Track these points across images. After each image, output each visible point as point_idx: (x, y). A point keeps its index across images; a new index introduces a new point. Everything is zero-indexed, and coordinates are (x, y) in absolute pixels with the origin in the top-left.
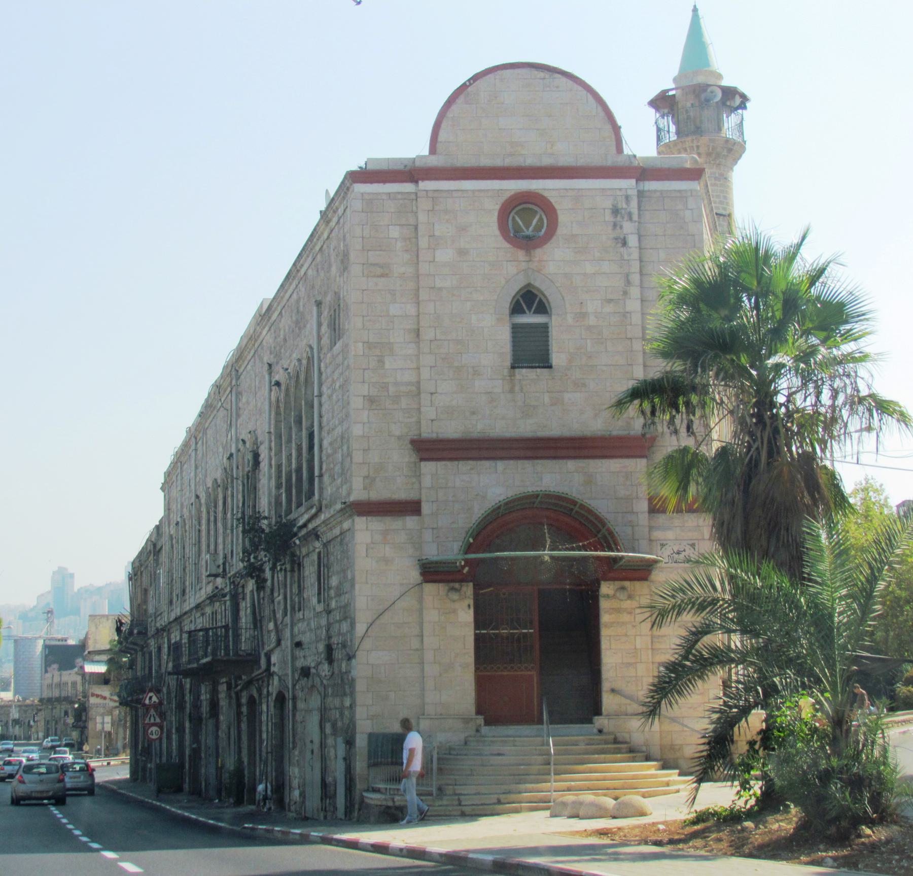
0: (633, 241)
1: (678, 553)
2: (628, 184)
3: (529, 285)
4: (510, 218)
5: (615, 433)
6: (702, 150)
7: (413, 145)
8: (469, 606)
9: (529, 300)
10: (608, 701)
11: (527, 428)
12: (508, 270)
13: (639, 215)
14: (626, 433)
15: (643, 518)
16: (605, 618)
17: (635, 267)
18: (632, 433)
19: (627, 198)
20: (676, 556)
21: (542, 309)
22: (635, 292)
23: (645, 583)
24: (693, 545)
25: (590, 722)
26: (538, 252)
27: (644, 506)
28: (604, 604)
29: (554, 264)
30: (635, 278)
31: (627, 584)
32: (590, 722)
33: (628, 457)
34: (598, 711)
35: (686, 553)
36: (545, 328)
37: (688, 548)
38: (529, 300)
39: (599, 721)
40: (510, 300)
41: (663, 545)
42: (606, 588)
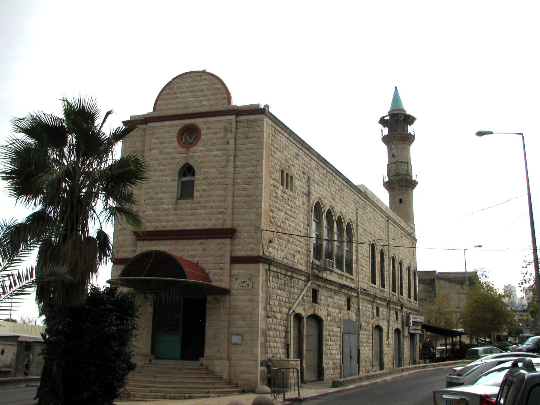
0: (232, 141)
1: (243, 282)
2: (232, 118)
3: (187, 164)
4: (184, 136)
5: (217, 227)
6: (396, 138)
7: (146, 108)
8: (151, 305)
9: (187, 170)
10: (208, 351)
11: (181, 226)
12: (178, 156)
13: (236, 131)
14: (222, 227)
15: (227, 266)
16: (208, 312)
17: (232, 153)
18: (225, 227)
19: (231, 123)
20: (242, 284)
21: (193, 174)
22: (231, 164)
23: (228, 296)
24: (250, 279)
25: (198, 360)
26: (192, 149)
27: (228, 260)
28: (208, 305)
29: (198, 154)
30: (232, 158)
31: (219, 297)
32: (198, 360)
33: (222, 238)
34: (203, 356)
35: (247, 283)
36: (193, 182)
37: (248, 280)
38: (187, 170)
39: (202, 360)
40: (178, 170)
41: (236, 279)
42: (209, 298)
